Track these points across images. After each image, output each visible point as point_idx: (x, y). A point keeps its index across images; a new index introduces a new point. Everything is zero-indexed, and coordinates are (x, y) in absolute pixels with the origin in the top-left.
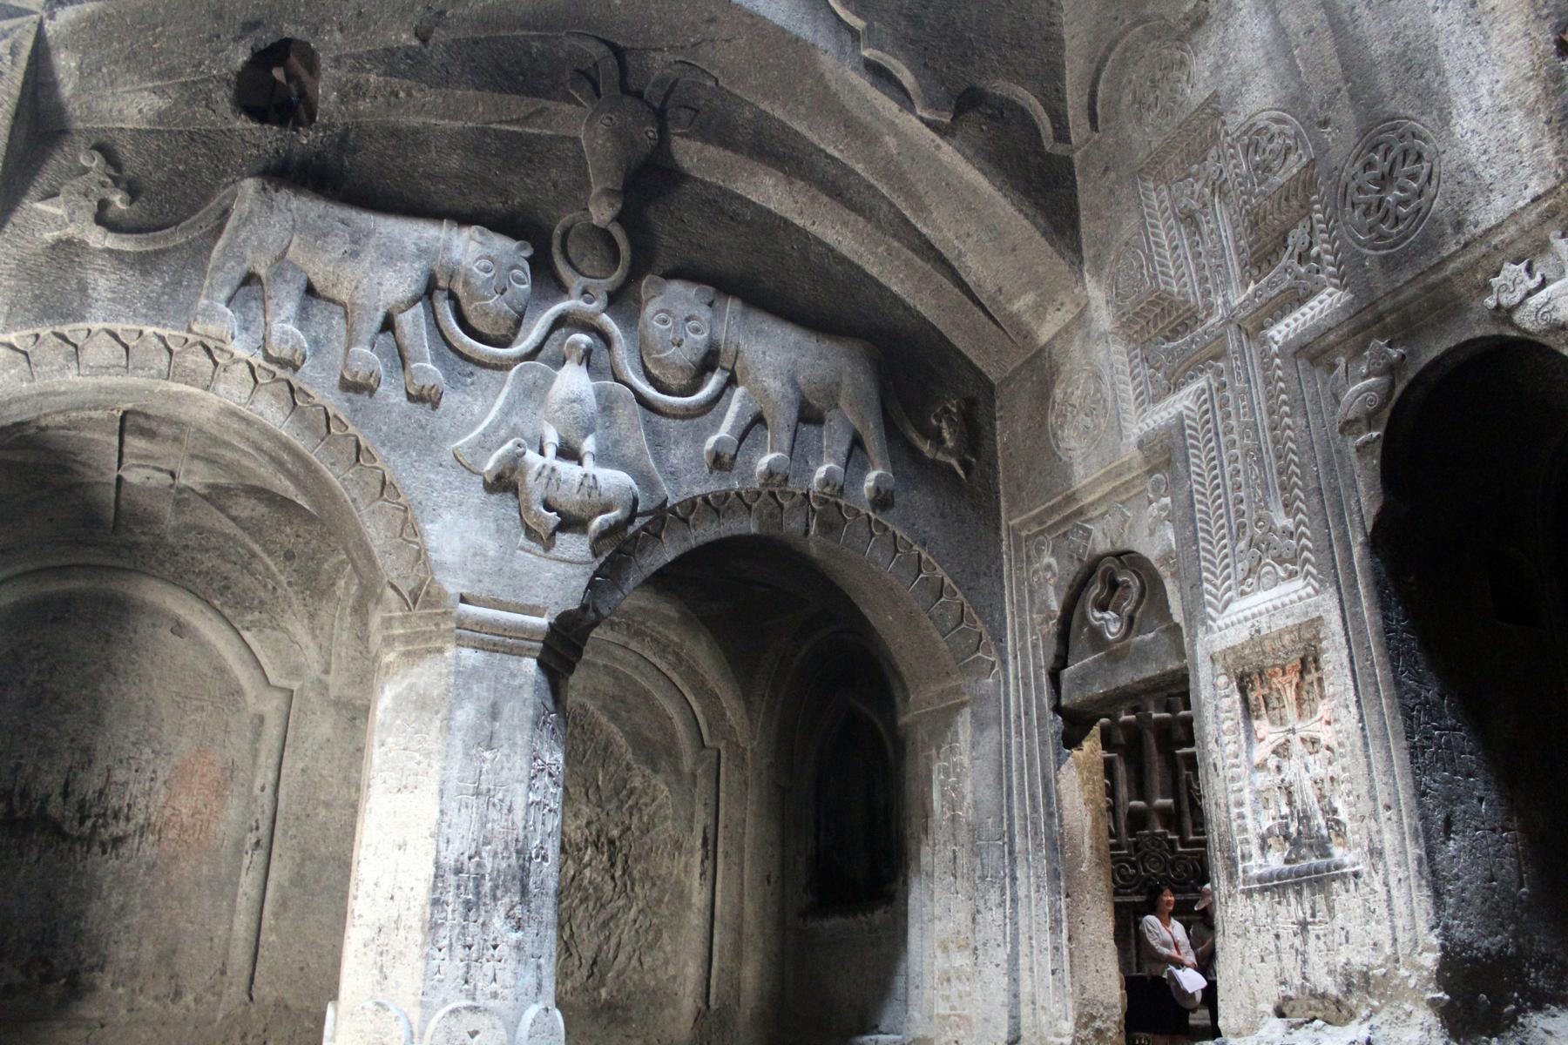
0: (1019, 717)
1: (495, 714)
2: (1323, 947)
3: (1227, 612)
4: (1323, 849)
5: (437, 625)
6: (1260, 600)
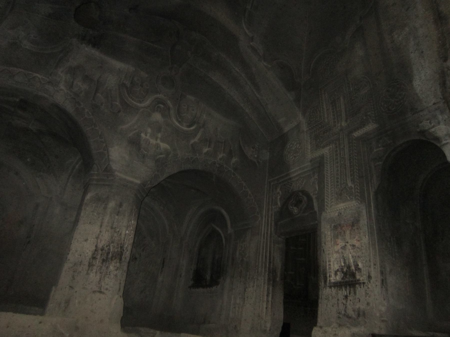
0: (264, 234)
1: (121, 205)
2: (352, 303)
4: (353, 275)
5: (108, 177)
6: (342, 206)
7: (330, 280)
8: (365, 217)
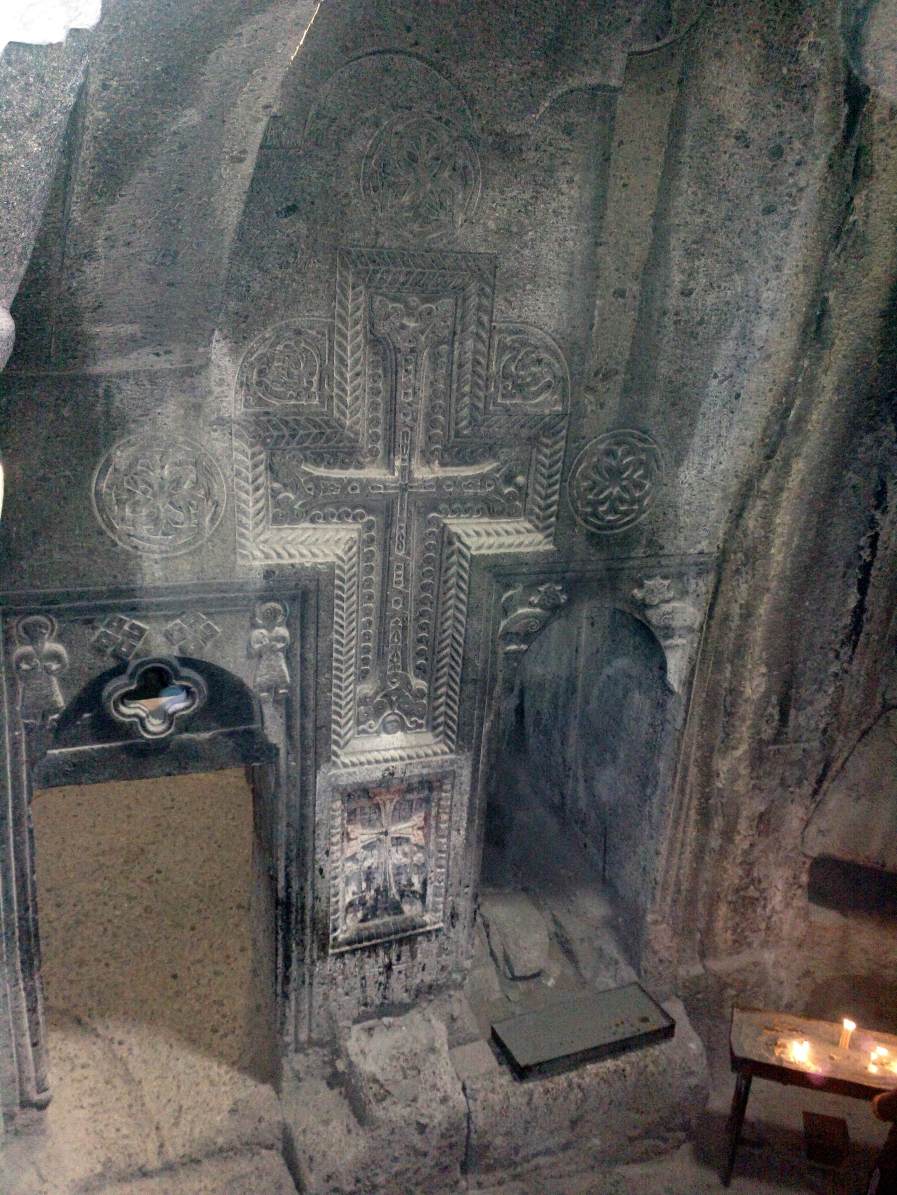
3: (345, 750)
7: (335, 939)
8: (466, 787)
